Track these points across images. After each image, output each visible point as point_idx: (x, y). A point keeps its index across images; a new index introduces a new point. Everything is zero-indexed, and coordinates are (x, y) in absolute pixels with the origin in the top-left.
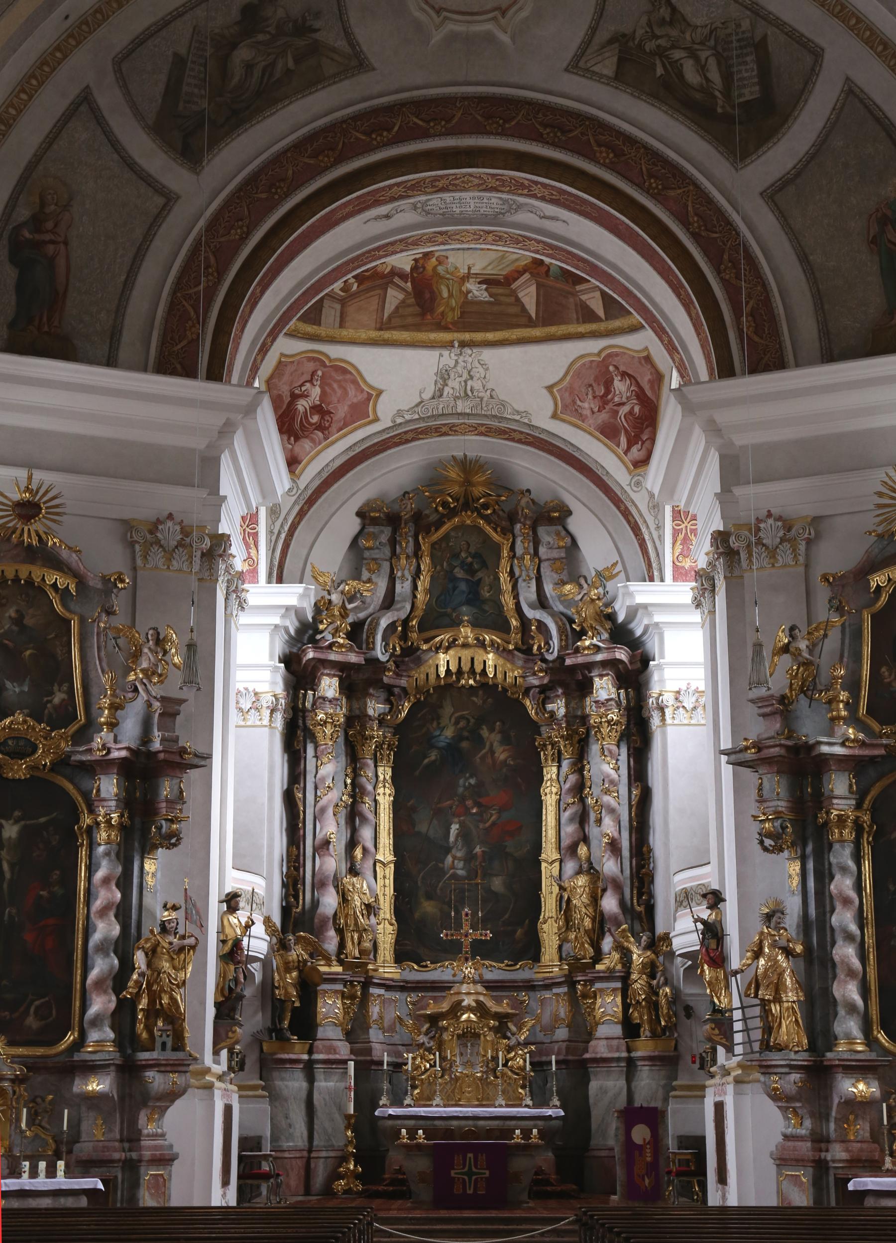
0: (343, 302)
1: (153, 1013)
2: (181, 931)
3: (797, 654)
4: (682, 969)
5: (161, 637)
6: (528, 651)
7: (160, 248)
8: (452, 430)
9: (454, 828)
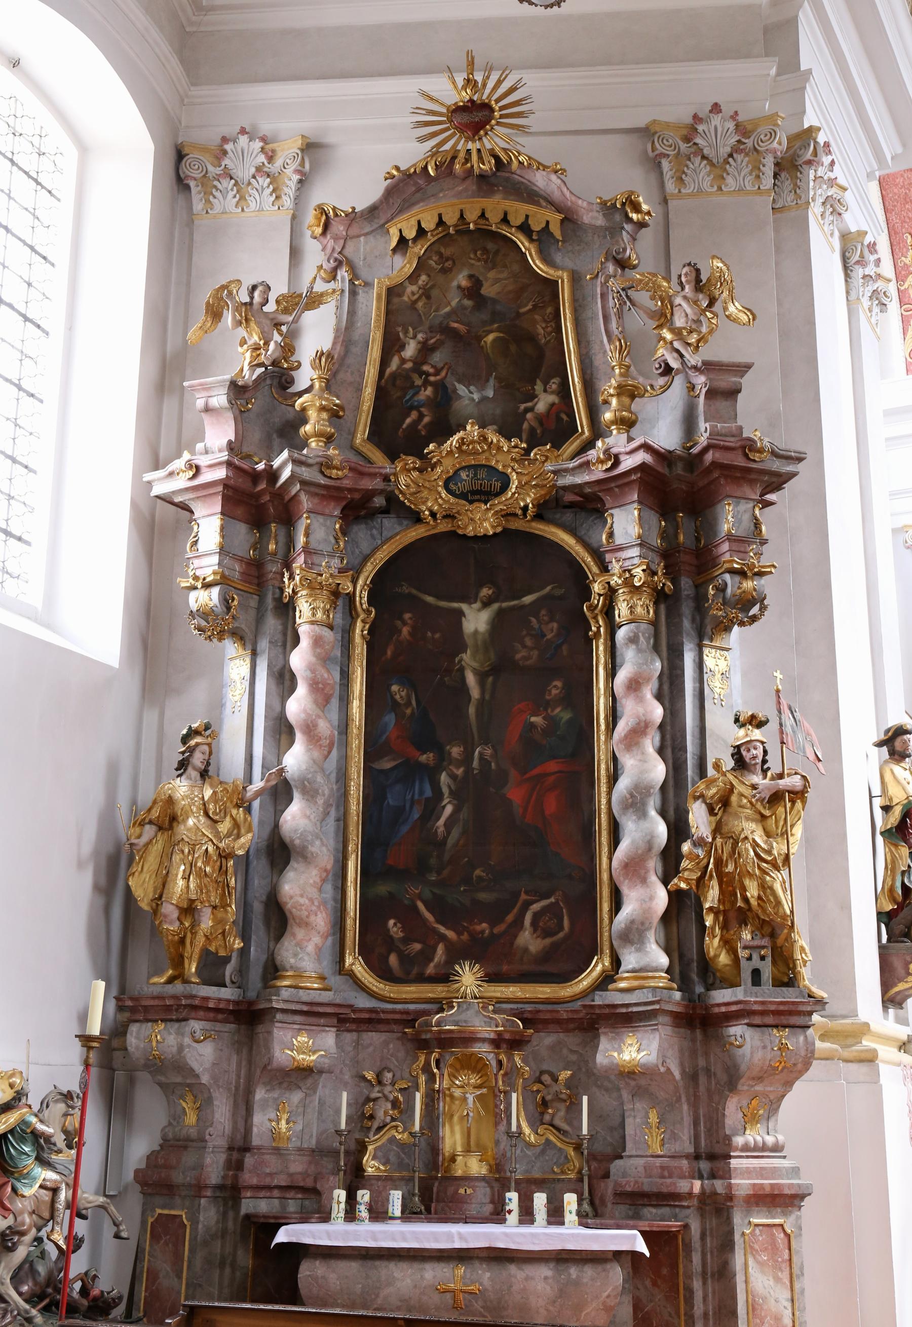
2: (774, 766)
5: (704, 278)
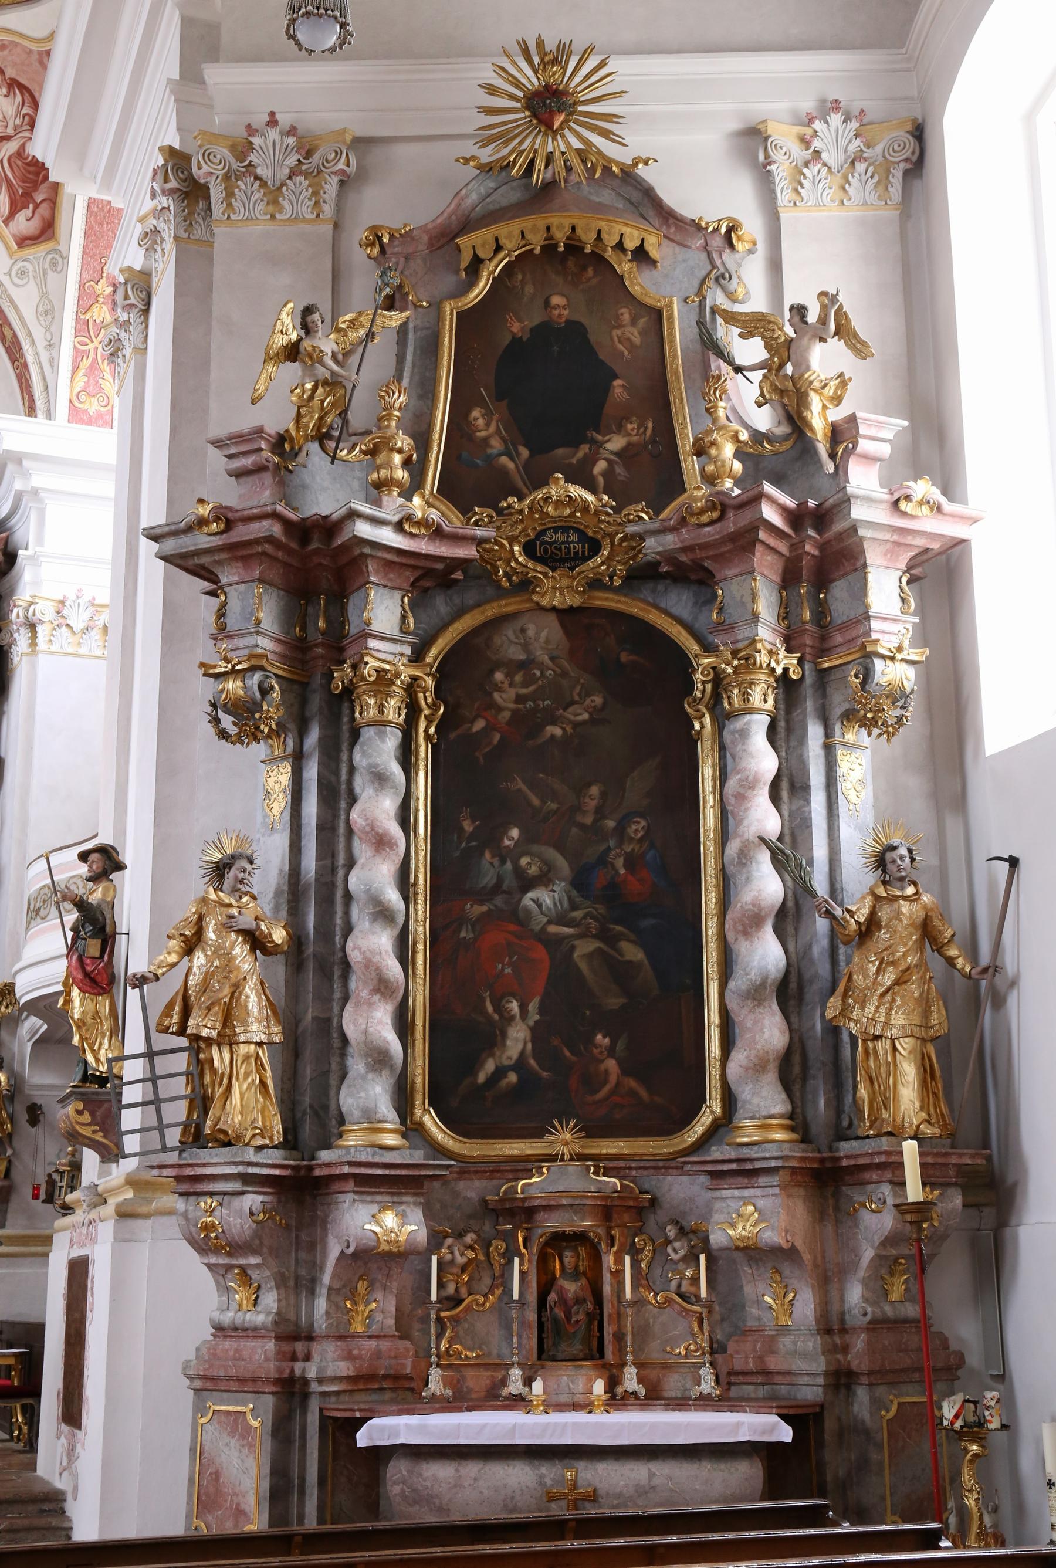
3: (315, 358)
4: (30, 1044)
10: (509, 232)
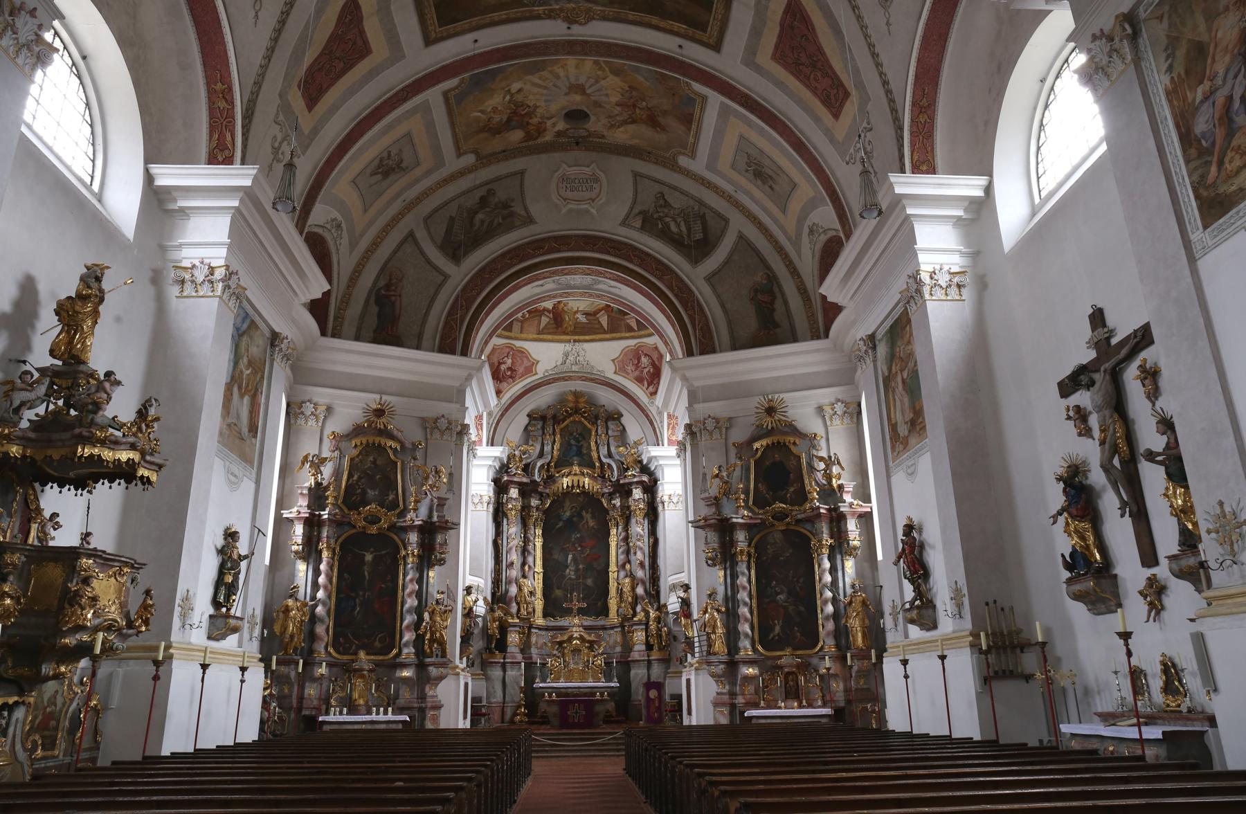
0: (522, 322)
1: (432, 641)
6: (603, 477)
7: (442, 297)
8: (570, 378)
9: (570, 557)
10: (764, 442)
